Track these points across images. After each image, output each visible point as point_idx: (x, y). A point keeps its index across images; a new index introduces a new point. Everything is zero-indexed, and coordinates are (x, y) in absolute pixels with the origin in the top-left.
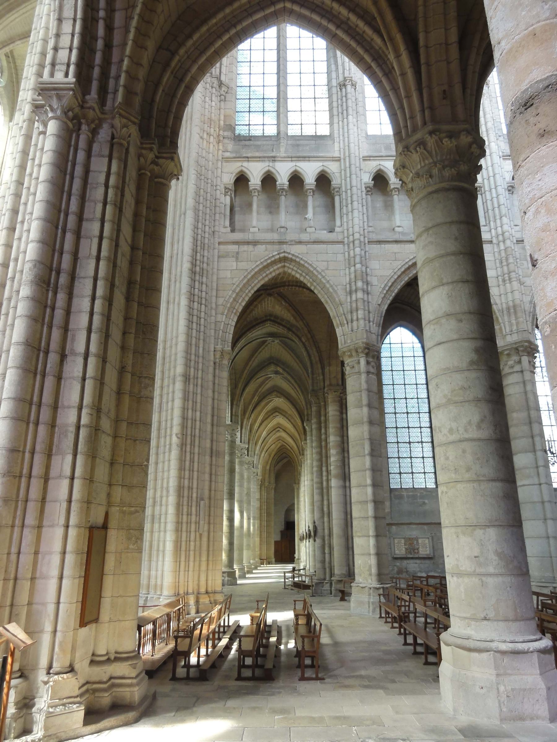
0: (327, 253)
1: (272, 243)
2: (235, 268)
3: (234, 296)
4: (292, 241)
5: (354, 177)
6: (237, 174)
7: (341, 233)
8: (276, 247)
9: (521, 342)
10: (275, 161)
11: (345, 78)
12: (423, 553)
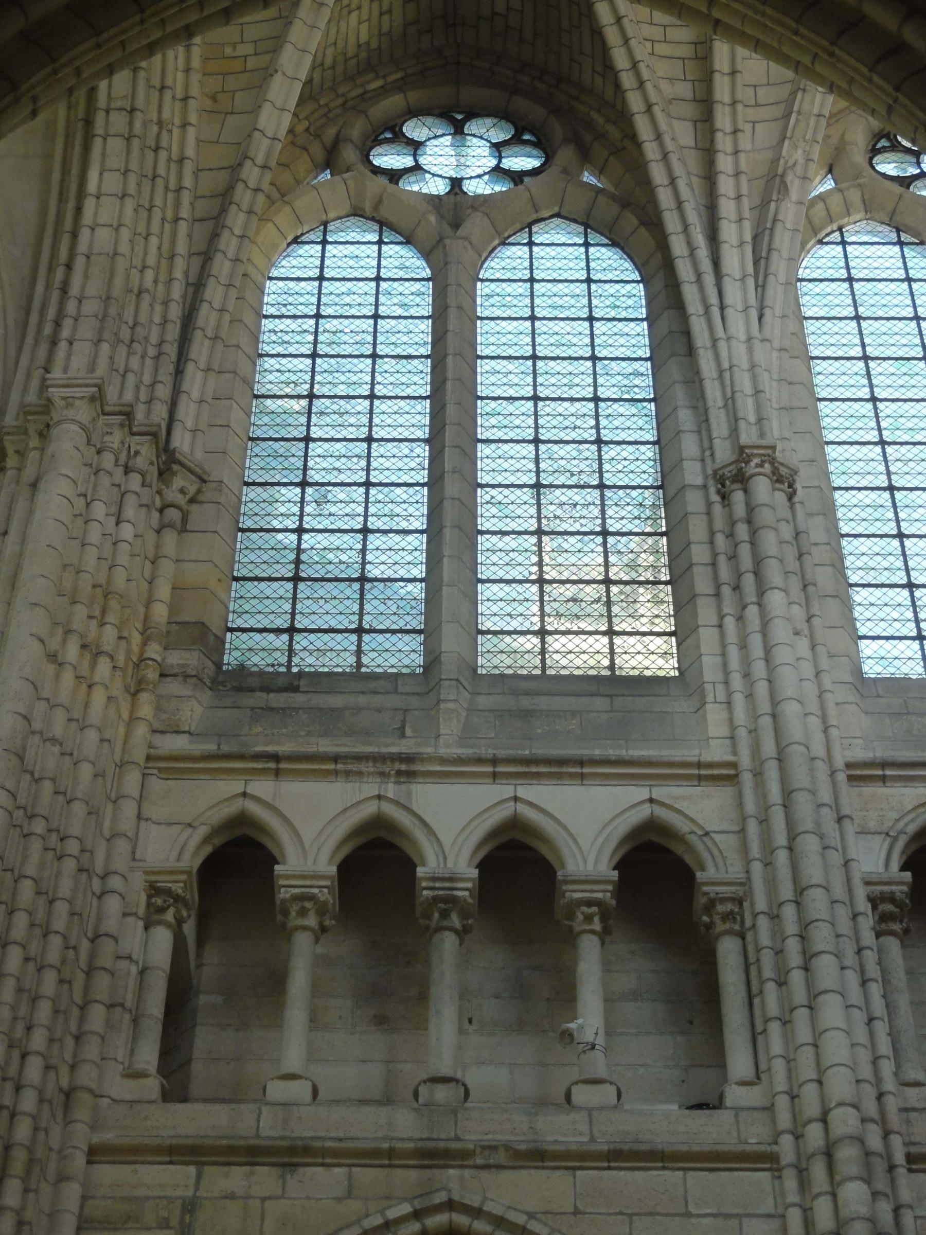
0: (688, 1215)
4: (494, 1148)
5: (810, 844)
6: (216, 831)
7: (757, 1115)
10: (411, 774)
11: (742, 449)
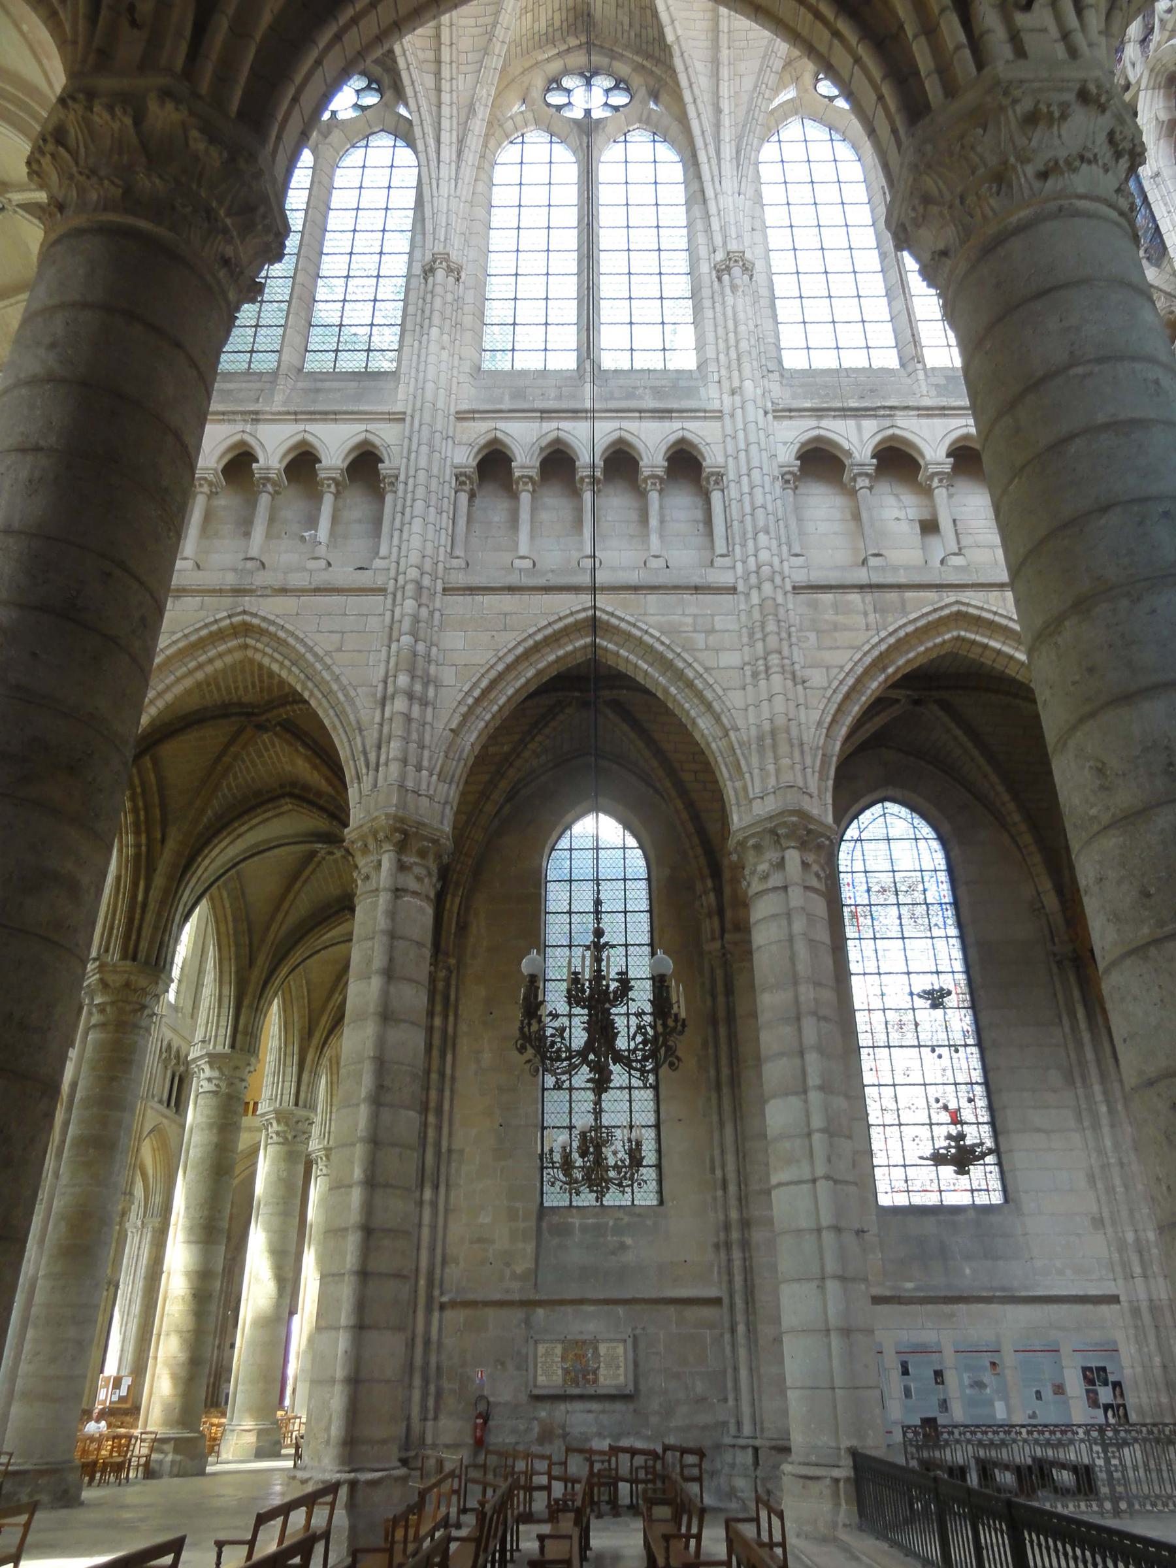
1: (219, 592)
8: (227, 601)
9: (781, 814)
10: (258, 420)
12: (608, 1382)
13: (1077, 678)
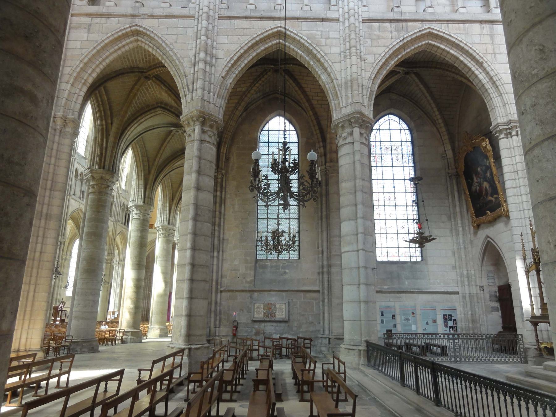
0: (178, 27)
1: (125, 16)
2: (85, 39)
3: (81, 65)
9: (353, 113)
12: (279, 317)
13: (533, 4)
